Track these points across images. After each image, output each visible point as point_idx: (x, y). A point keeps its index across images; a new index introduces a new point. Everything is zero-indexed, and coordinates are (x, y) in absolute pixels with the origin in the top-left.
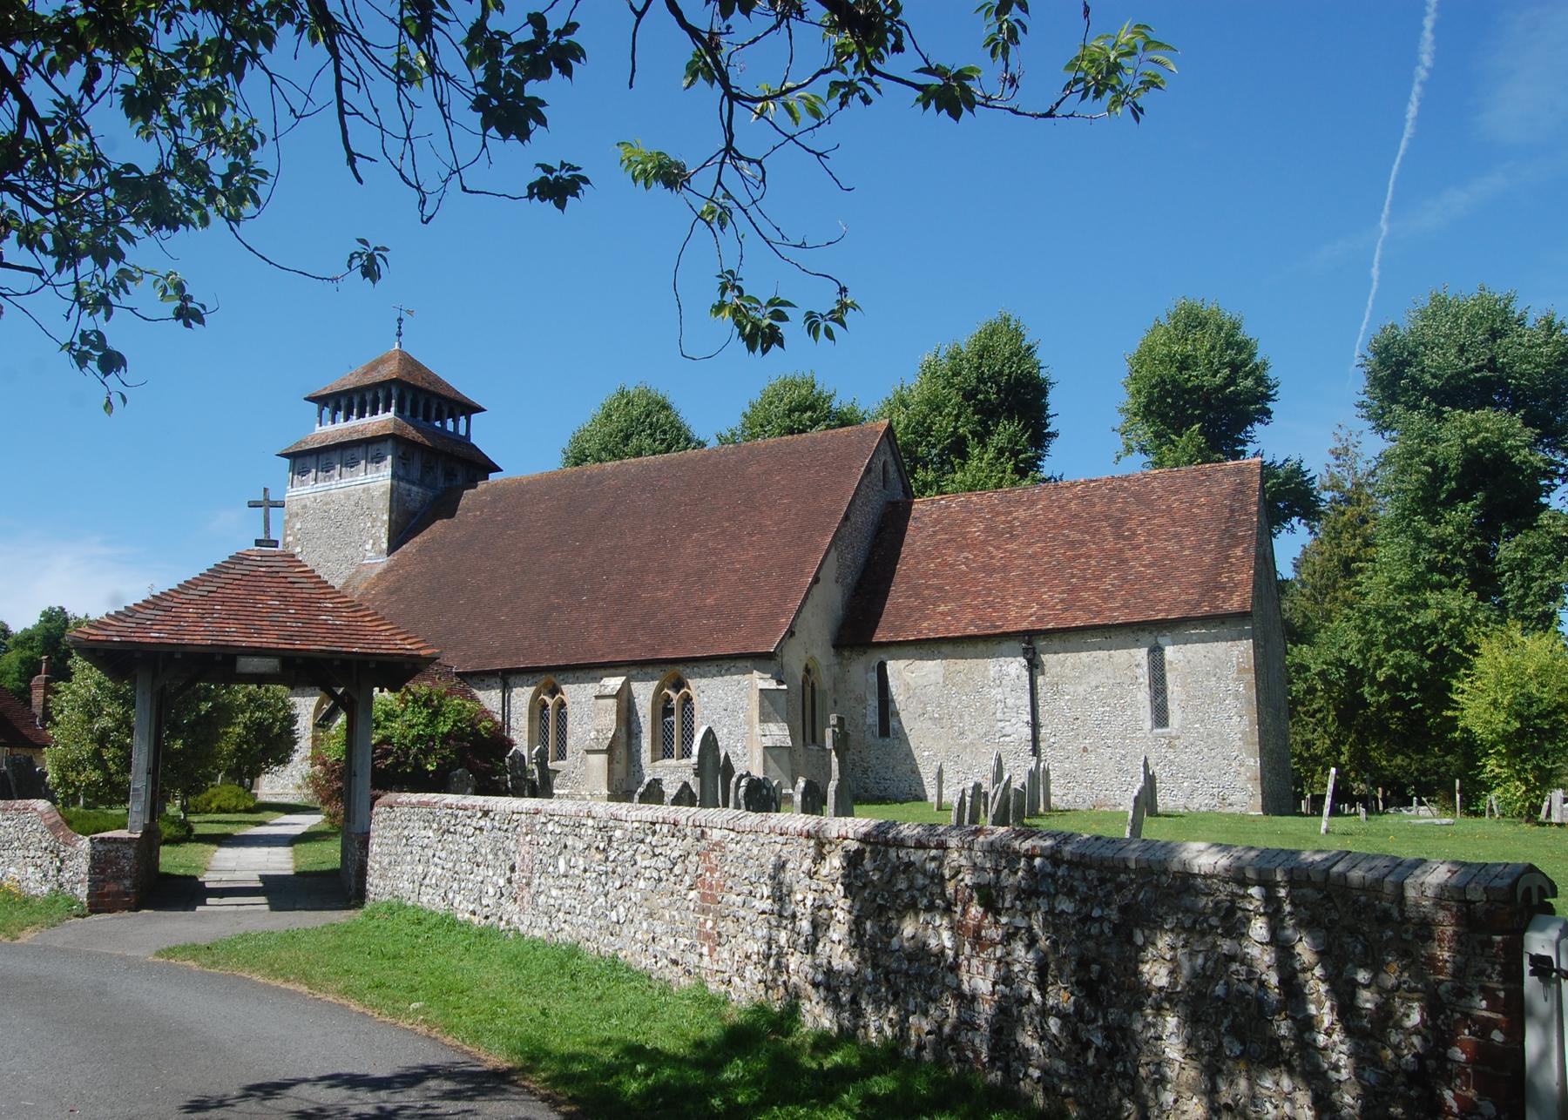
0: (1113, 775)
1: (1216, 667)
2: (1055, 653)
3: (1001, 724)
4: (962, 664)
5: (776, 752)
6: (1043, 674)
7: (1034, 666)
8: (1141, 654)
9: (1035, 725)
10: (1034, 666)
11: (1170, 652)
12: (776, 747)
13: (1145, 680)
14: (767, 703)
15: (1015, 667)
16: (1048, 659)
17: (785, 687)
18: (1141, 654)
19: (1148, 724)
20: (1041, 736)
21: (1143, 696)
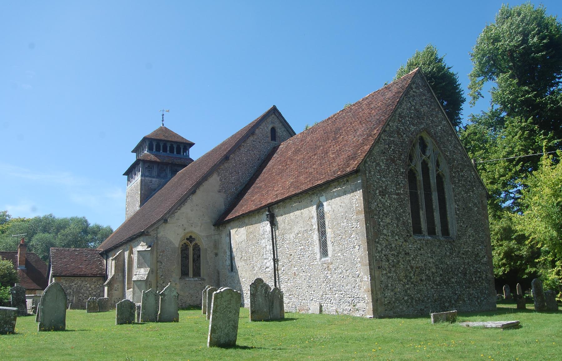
0: (306, 290)
1: (346, 212)
2: (282, 215)
3: (266, 261)
4: (251, 228)
5: (139, 283)
6: (278, 229)
7: (273, 224)
8: (313, 210)
9: (275, 261)
10: (273, 224)
11: (327, 206)
12: (138, 281)
13: (315, 227)
14: (141, 258)
15: (266, 226)
16: (279, 219)
17: (149, 249)
18: (313, 210)
19: (318, 256)
20: (279, 267)
21: (316, 236)
